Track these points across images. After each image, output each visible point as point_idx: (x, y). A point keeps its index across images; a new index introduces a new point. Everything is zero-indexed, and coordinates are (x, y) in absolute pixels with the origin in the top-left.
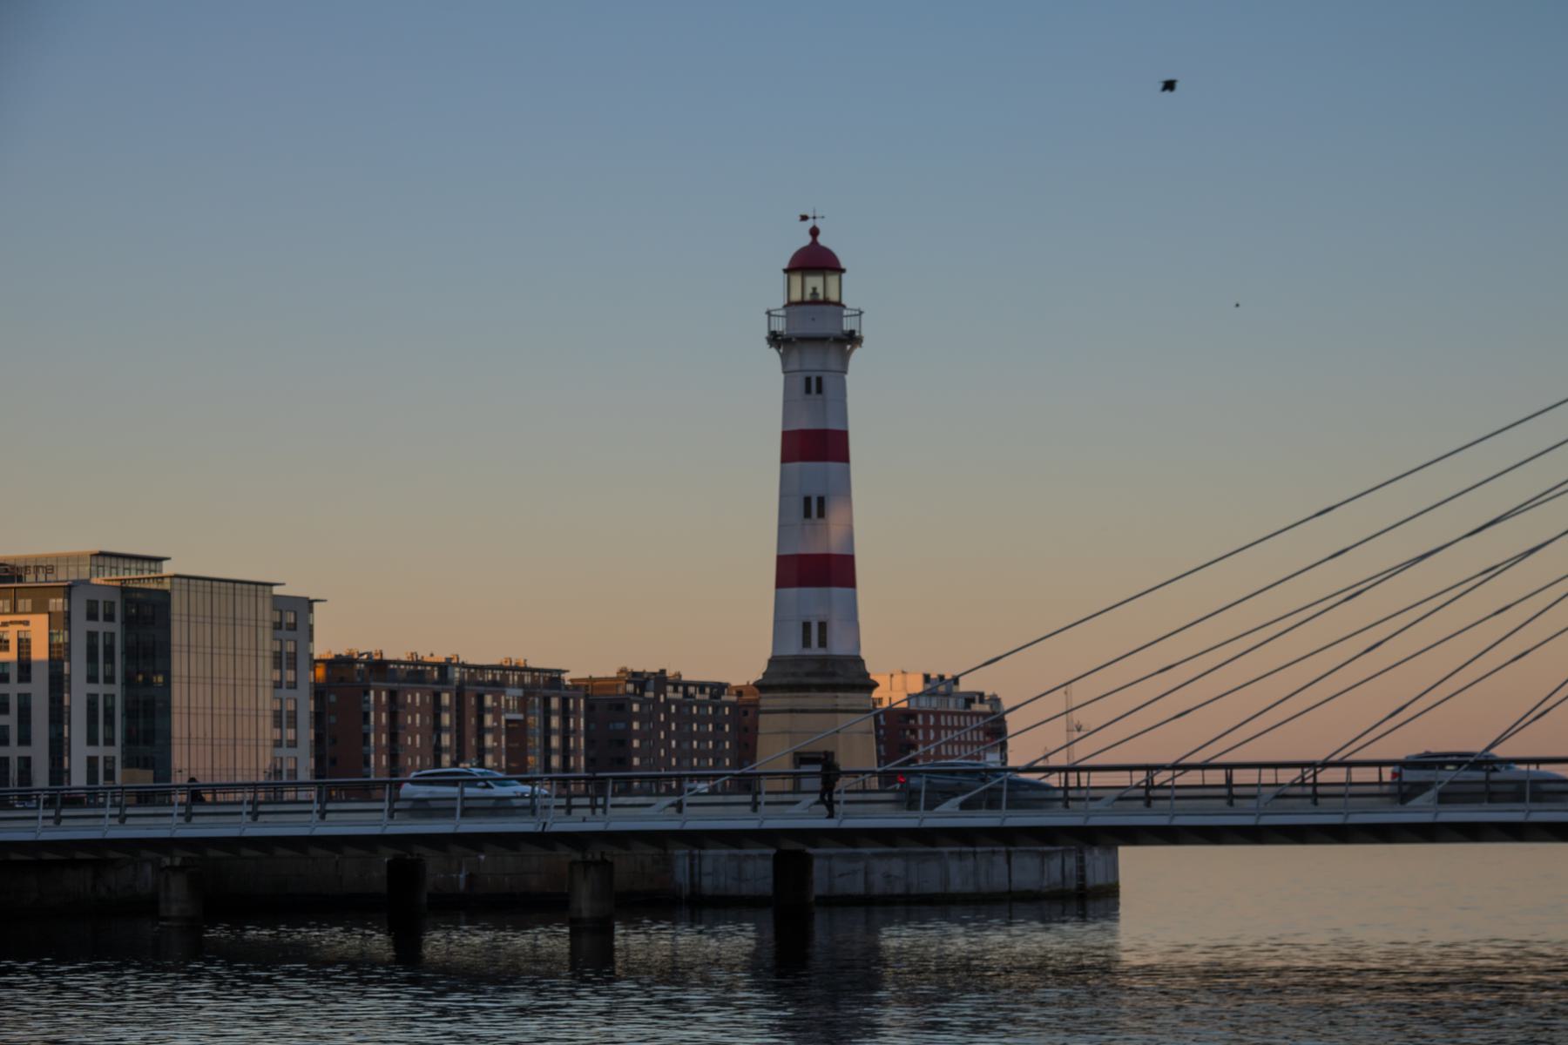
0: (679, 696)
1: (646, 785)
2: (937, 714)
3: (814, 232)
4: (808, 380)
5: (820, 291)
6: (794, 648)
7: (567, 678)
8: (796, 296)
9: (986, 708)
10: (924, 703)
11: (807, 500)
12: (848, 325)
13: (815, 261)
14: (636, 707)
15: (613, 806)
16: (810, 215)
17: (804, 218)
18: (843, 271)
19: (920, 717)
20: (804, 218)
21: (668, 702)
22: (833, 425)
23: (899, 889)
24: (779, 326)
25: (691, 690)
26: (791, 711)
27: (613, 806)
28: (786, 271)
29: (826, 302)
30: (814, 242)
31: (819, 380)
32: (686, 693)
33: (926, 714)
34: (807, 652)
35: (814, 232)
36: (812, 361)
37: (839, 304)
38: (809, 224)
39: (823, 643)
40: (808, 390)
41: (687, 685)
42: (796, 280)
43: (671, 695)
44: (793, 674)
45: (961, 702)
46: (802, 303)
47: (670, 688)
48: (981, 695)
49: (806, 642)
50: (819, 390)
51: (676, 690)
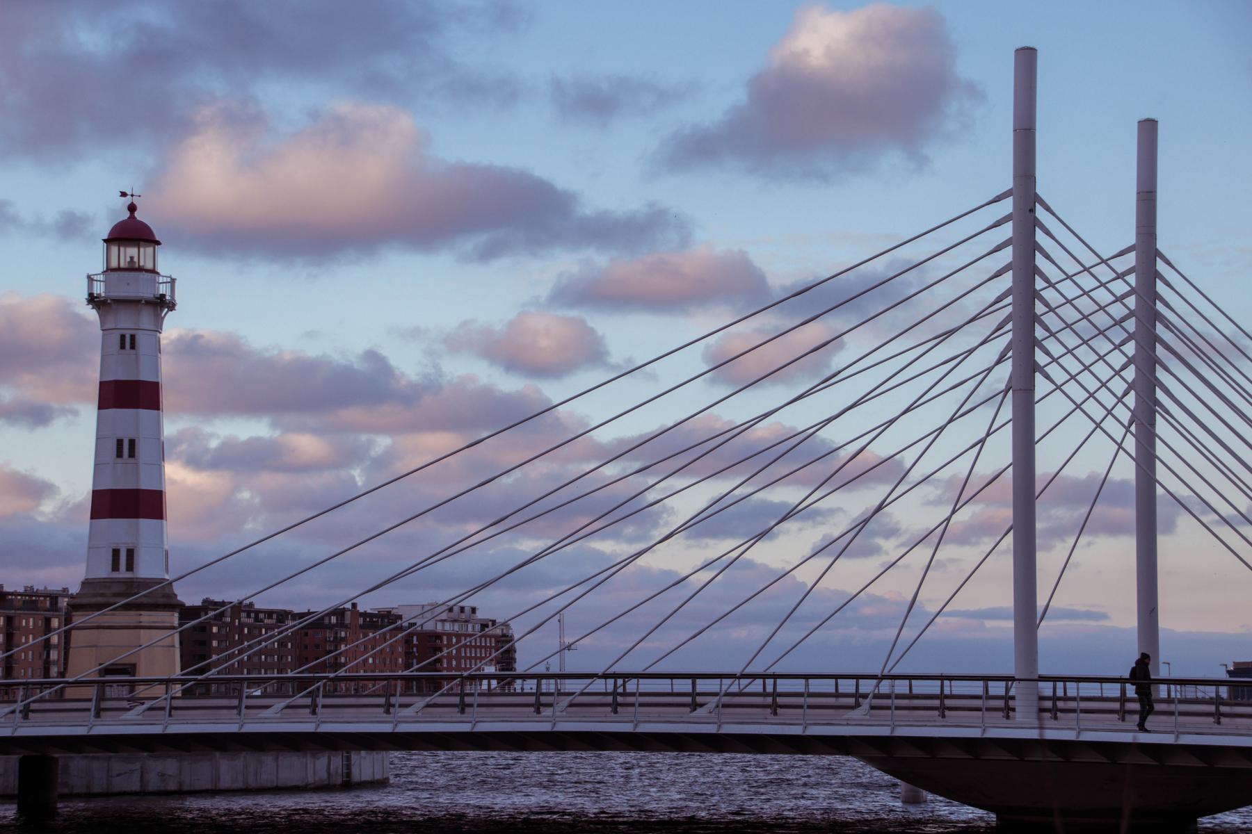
0: (251, 621)
1: (223, 689)
2: (459, 636)
3: (132, 208)
4: (123, 337)
5: (136, 259)
6: (103, 571)
7: (480, 615)
8: (114, 264)
9: (498, 632)
10: (448, 627)
11: (120, 443)
12: (163, 289)
13: (131, 233)
14: (215, 630)
15: (247, 707)
16: (129, 193)
17: (124, 194)
18: (158, 243)
19: (445, 638)
20: (124, 194)
21: (242, 625)
22: (145, 376)
23: (172, 786)
24: (99, 289)
25: (261, 616)
26: (98, 628)
27: (247, 707)
28: (105, 241)
29: (140, 269)
30: (132, 217)
31: (133, 337)
32: (257, 619)
33: (449, 636)
34: (116, 575)
35: (132, 208)
36: (125, 321)
37: (153, 271)
38: (128, 200)
39: (130, 567)
40: (123, 346)
41: (257, 612)
42: (114, 249)
43: (244, 619)
44: (102, 595)
45: (478, 627)
46: (119, 269)
47: (243, 615)
48: (494, 622)
49: (115, 567)
50: (133, 346)
51: (249, 616)
